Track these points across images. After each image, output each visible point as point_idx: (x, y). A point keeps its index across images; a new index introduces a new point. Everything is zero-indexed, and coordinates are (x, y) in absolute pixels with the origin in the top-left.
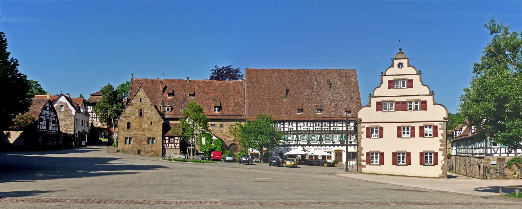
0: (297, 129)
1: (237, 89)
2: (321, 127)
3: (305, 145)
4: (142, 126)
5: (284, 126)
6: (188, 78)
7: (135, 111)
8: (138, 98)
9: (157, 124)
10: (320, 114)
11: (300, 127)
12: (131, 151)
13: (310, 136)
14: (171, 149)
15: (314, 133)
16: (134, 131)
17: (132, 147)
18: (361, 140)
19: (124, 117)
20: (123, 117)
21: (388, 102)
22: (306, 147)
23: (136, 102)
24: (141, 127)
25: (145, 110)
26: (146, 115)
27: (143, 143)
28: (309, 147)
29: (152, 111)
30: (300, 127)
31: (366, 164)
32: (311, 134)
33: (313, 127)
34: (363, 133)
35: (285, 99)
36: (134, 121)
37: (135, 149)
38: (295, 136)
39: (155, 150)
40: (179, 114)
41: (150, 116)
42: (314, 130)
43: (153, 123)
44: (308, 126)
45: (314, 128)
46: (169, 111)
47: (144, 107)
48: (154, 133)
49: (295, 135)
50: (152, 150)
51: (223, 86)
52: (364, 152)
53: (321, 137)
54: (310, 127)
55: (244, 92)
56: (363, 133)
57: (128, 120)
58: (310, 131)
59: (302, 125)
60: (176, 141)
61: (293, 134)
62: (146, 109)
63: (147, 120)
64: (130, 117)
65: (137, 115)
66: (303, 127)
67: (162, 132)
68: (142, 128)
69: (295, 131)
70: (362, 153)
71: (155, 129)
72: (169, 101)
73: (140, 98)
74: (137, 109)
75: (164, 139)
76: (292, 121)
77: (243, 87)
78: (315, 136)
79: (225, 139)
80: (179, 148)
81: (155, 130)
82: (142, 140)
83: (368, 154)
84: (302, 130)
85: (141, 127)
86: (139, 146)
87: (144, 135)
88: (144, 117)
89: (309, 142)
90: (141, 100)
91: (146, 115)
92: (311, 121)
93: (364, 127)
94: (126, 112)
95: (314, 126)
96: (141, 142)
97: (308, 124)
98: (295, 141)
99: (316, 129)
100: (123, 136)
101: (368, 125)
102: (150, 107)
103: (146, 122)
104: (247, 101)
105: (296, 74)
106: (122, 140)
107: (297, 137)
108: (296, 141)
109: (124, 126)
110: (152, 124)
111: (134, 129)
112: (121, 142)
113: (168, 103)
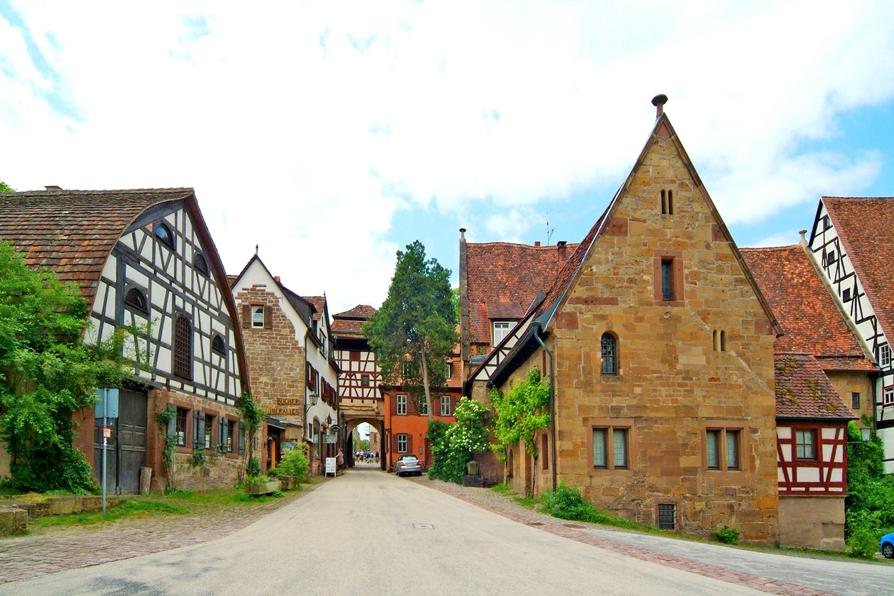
4: (676, 358)
9: (746, 346)
14: (808, 494)
16: (638, 390)
20: (579, 300)
24: (672, 366)
27: (685, 462)
29: (720, 270)
37: (650, 502)
39: (744, 506)
43: (732, 338)
47: (681, 245)
50: (731, 507)
57: (603, 317)
60: (827, 450)
64: (613, 301)
65: (650, 288)
67: (773, 393)
68: (679, 367)
71: (742, 376)
73: (659, 188)
80: (840, 490)
82: (680, 442)
86: (662, 482)
87: (689, 411)
88: (686, 301)
91: (693, 294)
102: (712, 245)
103: (694, 336)
106: (579, 441)
110: (723, 349)
111: (639, 374)
112: (572, 454)
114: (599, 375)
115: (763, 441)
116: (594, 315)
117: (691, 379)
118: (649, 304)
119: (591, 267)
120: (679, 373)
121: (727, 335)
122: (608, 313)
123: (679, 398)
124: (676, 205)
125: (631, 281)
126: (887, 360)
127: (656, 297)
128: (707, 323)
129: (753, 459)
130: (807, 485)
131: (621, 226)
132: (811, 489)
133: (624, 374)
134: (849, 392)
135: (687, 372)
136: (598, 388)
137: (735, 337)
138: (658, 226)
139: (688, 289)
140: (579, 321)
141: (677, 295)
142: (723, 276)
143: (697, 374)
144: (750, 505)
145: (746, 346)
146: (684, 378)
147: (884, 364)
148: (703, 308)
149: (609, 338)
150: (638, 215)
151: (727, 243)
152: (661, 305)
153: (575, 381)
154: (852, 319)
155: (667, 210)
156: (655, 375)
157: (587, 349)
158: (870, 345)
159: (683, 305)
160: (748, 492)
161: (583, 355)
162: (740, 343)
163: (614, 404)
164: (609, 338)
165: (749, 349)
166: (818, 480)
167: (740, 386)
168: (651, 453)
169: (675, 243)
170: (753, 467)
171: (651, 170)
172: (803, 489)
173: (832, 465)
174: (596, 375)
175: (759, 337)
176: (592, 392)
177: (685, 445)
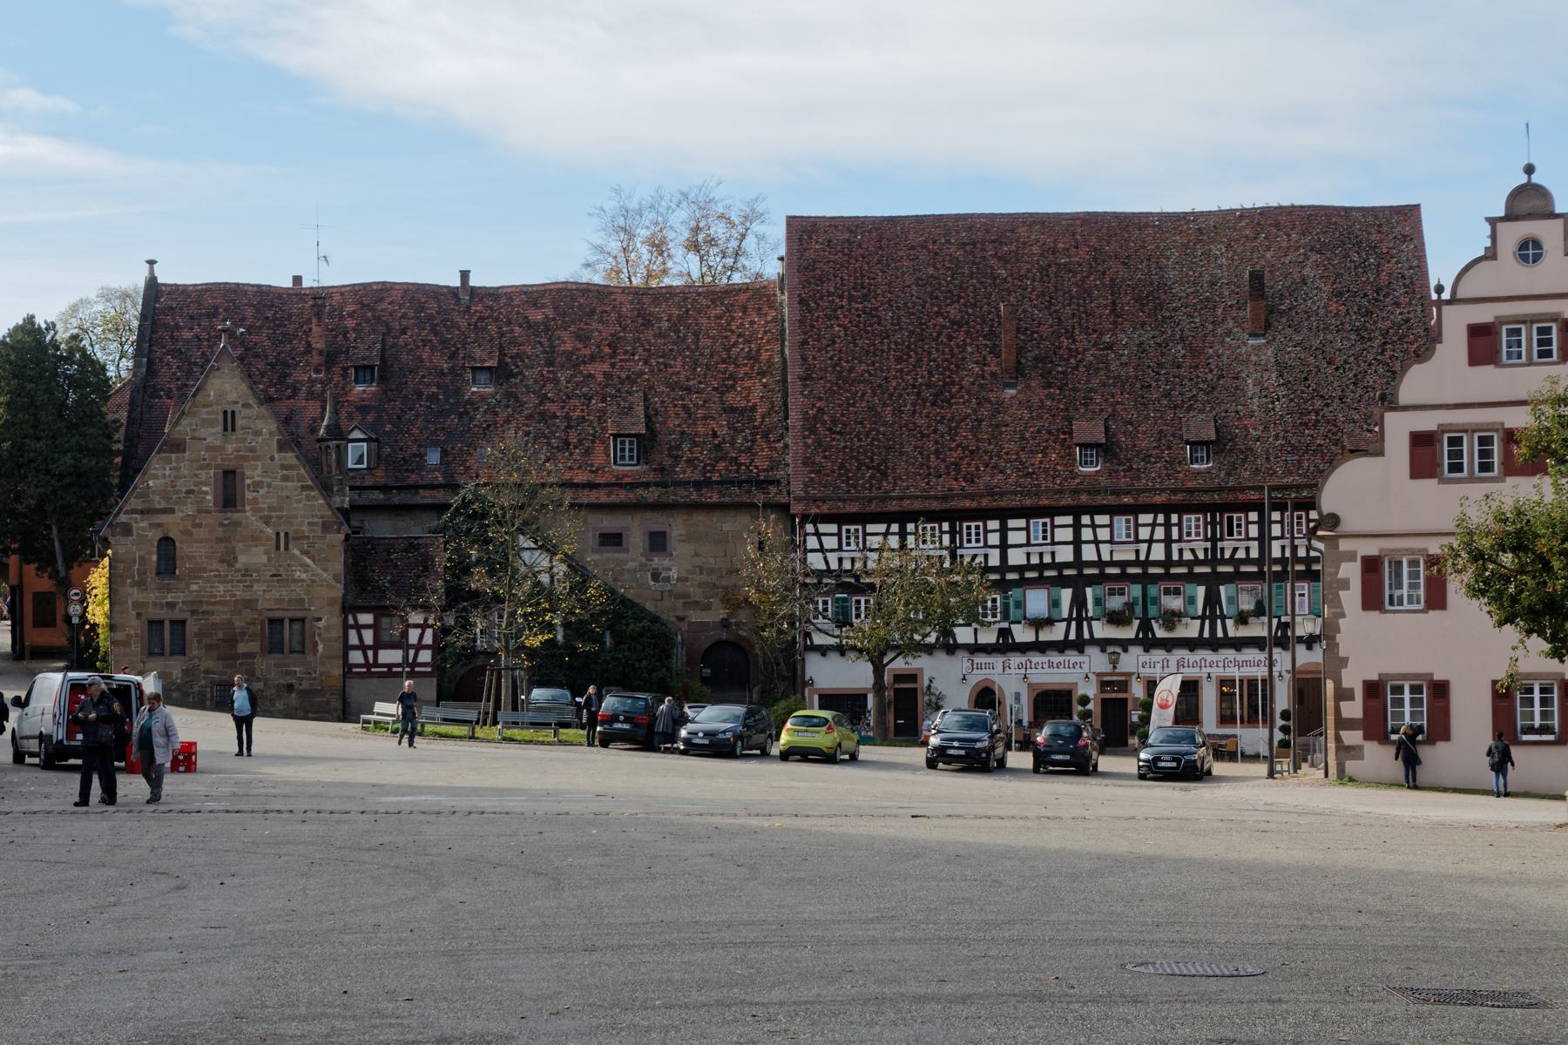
0: (1078, 552)
1: (739, 336)
2: (1214, 540)
3: (1125, 644)
4: (235, 559)
5: (1004, 538)
6: (465, 275)
7: (196, 475)
8: (215, 408)
9: (311, 545)
10: (1208, 471)
11: (1096, 542)
12: (178, 689)
13: (1153, 590)
15: (1170, 575)
16: (194, 587)
17: (186, 672)
18: (1341, 621)
19: (142, 512)
20: (134, 511)
21: (1470, 433)
22: (1126, 650)
23: (203, 433)
24: (230, 565)
25: (253, 473)
26: (255, 500)
27: (242, 648)
28: (1146, 651)
29: (285, 478)
30: (1093, 546)
31: (1366, 738)
32: (1155, 579)
33: (1168, 541)
34: (1345, 584)
35: (1008, 386)
36: (191, 534)
38: (1066, 595)
39: (305, 685)
40: (420, 482)
41: (274, 501)
42: (1175, 557)
43: (295, 539)
44: (1141, 538)
45: (1175, 547)
46: (365, 466)
47: (244, 458)
48: (299, 591)
49: (1065, 587)
51: (659, 320)
52: (1353, 678)
53: (1212, 600)
54: (1151, 541)
55: (782, 352)
56: (1345, 584)
57: (159, 525)
58: (1147, 563)
59: (1103, 534)
60: (414, 636)
61: (1053, 586)
62: (256, 468)
64: (172, 511)
65: (208, 497)
66: (1111, 542)
67: (340, 587)
68: (238, 566)
69: (1067, 565)
70: (1346, 684)
71: (306, 571)
72: (364, 409)
74: (208, 467)
75: (351, 621)
76: (1051, 512)
77: (775, 320)
78: (1177, 592)
79: (680, 613)
80: (429, 669)
81: (304, 576)
83: (1373, 690)
84: (1106, 557)
85: (230, 565)
87: (248, 604)
88: (248, 508)
89: (1145, 626)
90: (229, 421)
91: (255, 500)
92: (1153, 509)
93: (1350, 556)
94: (151, 483)
95: (1175, 536)
96: (232, 641)
97: (1137, 526)
98: (1069, 620)
99: (1181, 551)
100: (139, 615)
101: (1371, 548)
102: (277, 456)
103: (255, 539)
104: (796, 403)
105: (1076, 241)
107: (1079, 602)
108: (1074, 623)
109: (142, 558)
110: (287, 548)
111: (195, 573)
113: (355, 423)
114: (154, 575)
115: (327, 628)
117: (251, 576)
120: (238, 571)
121: (291, 535)
122: (165, 521)
123: (238, 593)
124: (239, 422)
125: (189, 492)
129: (316, 644)
130: (390, 666)
131: (179, 445)
132: (395, 669)
135: (246, 570)
136: (154, 586)
137: (300, 537)
138: (218, 443)
141: (238, 503)
142: (285, 484)
143: (257, 571)
144: (311, 684)
145: (311, 545)
146: (243, 575)
149: (166, 543)
150: (197, 434)
153: (129, 581)
155: (230, 429)
157: (142, 553)
159: (244, 511)
160: (310, 673)
163: (169, 600)
164: (166, 543)
167: (303, 581)
168: (207, 641)
169: (236, 456)
170: (315, 651)
171: (212, 393)
172: (385, 669)
173: (420, 647)
176: (146, 589)
177: (244, 634)
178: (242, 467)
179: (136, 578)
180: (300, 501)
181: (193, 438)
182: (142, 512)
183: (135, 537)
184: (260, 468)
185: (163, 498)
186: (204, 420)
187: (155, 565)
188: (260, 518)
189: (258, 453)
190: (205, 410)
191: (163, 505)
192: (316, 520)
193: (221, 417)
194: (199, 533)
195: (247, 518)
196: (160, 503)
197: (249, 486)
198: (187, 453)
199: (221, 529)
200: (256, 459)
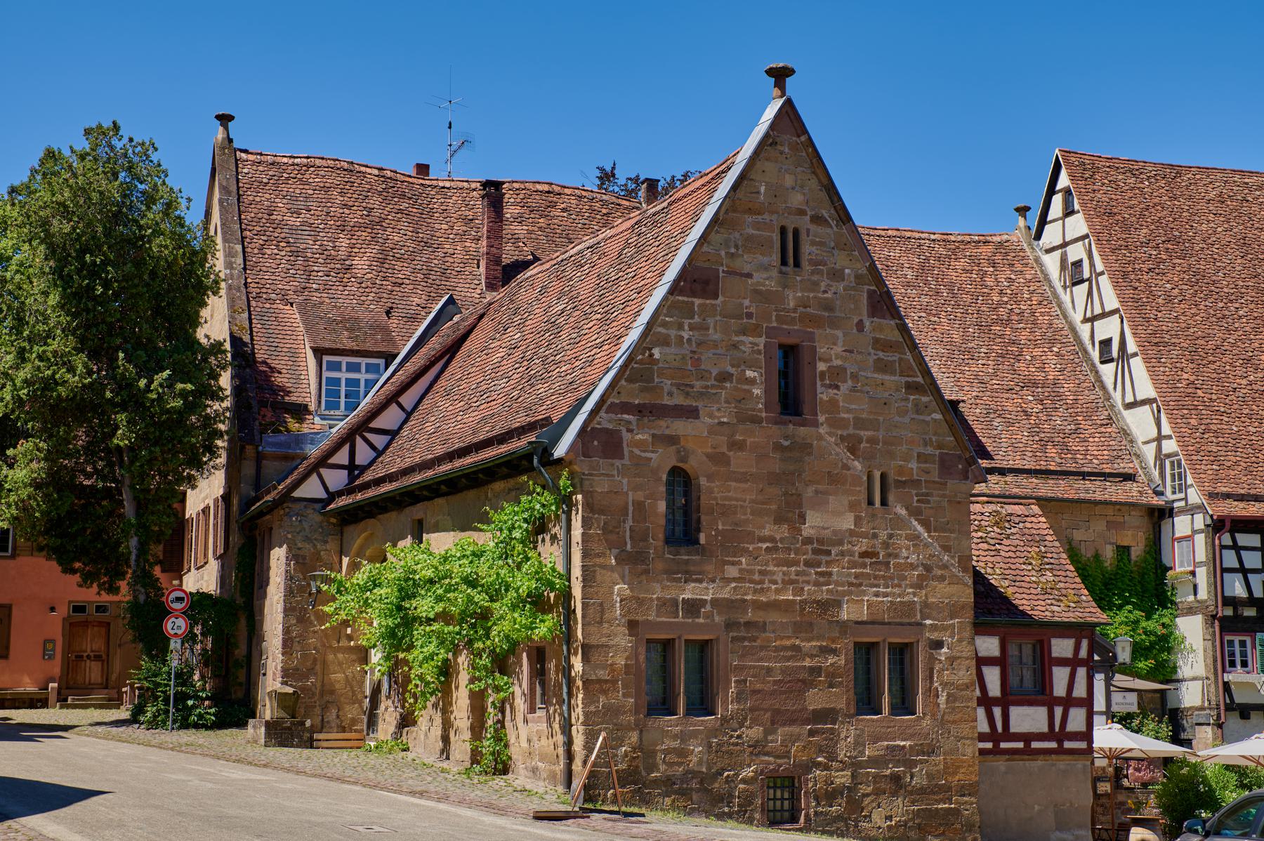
7: (735, 346)
14: (1028, 752)
19: (640, 410)
23: (746, 262)
26: (833, 403)
29: (882, 367)
57: (672, 440)
60: (1060, 676)
63: (842, 452)
64: (692, 413)
68: (807, 530)
73: (777, 221)
74: (755, 331)
88: (821, 418)
91: (833, 403)
94: (657, 353)
102: (867, 324)
103: (835, 479)
109: (639, 506)
110: (884, 503)
114: (660, 543)
116: (654, 436)
117: (828, 553)
118: (756, 420)
119: (650, 349)
120: (808, 541)
121: (892, 476)
122: (680, 433)
124: (807, 249)
125: (724, 377)
126: (1180, 485)
127: (767, 407)
128: (857, 457)
130: (1027, 738)
131: (707, 282)
132: (1035, 745)
133: (707, 544)
134: (1110, 543)
135: (820, 541)
136: (660, 566)
138: (772, 285)
139: (825, 398)
140: (625, 445)
141: (806, 408)
142: (887, 377)
147: (1174, 493)
148: (851, 431)
150: (738, 264)
151: (892, 323)
152: (776, 423)
154: (1117, 396)
155: (791, 261)
156: (765, 546)
157: (640, 496)
158: (1149, 452)
159: (816, 424)
161: (631, 508)
162: (914, 492)
165: (928, 502)
166: (1045, 729)
171: (763, 189)
172: (1020, 745)
174: (656, 542)
175: (945, 484)
176: (647, 572)
178: (811, 337)
179: (629, 547)
180: (901, 413)
181: (732, 273)
182: (640, 410)
183: (626, 461)
184: (840, 343)
185: (678, 386)
186: (749, 238)
187: (662, 521)
188: (842, 438)
189: (838, 314)
190: (749, 219)
191: (678, 400)
192: (929, 450)
193: (776, 237)
194: (740, 462)
195: (820, 438)
196: (670, 394)
197: (822, 374)
198: (721, 298)
199: (777, 456)
200: (834, 324)
